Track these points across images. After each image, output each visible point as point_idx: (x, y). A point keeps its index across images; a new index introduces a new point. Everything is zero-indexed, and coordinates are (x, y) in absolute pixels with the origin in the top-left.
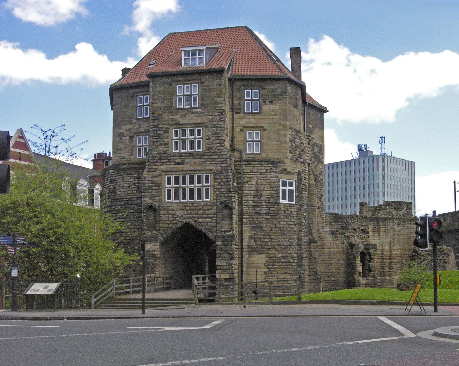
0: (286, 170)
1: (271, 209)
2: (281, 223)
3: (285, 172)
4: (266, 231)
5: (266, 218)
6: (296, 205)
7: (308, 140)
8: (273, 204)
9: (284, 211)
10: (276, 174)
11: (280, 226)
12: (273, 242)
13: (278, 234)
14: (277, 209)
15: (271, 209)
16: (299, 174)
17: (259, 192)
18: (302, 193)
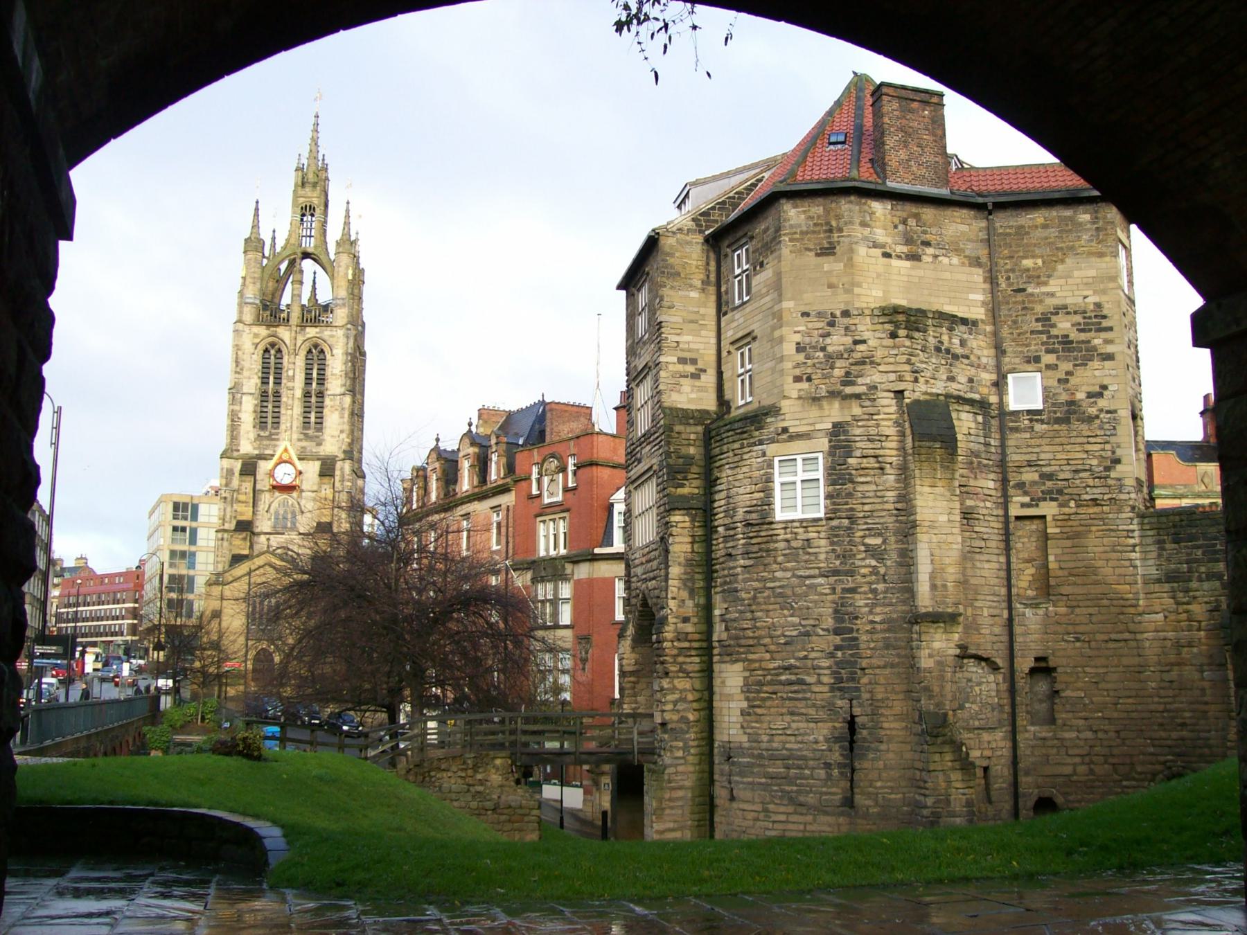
0: (785, 430)
1: (754, 541)
2: (778, 574)
3: (785, 436)
4: (744, 600)
5: (745, 567)
6: (831, 519)
7: (889, 327)
8: (757, 528)
9: (787, 541)
10: (760, 447)
11: (772, 585)
12: (758, 628)
13: (771, 607)
14: (765, 539)
15: (754, 541)
16: (838, 429)
17: (731, 501)
18: (852, 482)
